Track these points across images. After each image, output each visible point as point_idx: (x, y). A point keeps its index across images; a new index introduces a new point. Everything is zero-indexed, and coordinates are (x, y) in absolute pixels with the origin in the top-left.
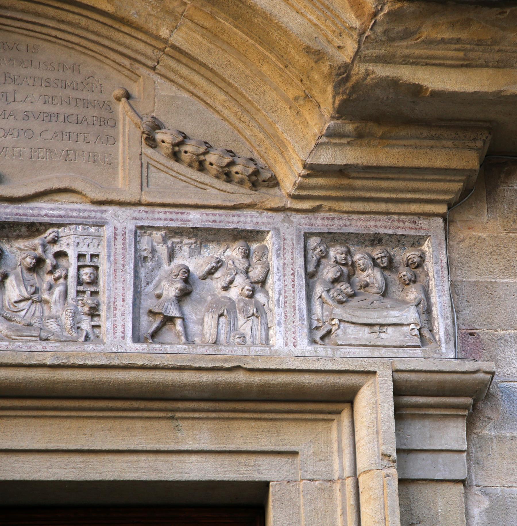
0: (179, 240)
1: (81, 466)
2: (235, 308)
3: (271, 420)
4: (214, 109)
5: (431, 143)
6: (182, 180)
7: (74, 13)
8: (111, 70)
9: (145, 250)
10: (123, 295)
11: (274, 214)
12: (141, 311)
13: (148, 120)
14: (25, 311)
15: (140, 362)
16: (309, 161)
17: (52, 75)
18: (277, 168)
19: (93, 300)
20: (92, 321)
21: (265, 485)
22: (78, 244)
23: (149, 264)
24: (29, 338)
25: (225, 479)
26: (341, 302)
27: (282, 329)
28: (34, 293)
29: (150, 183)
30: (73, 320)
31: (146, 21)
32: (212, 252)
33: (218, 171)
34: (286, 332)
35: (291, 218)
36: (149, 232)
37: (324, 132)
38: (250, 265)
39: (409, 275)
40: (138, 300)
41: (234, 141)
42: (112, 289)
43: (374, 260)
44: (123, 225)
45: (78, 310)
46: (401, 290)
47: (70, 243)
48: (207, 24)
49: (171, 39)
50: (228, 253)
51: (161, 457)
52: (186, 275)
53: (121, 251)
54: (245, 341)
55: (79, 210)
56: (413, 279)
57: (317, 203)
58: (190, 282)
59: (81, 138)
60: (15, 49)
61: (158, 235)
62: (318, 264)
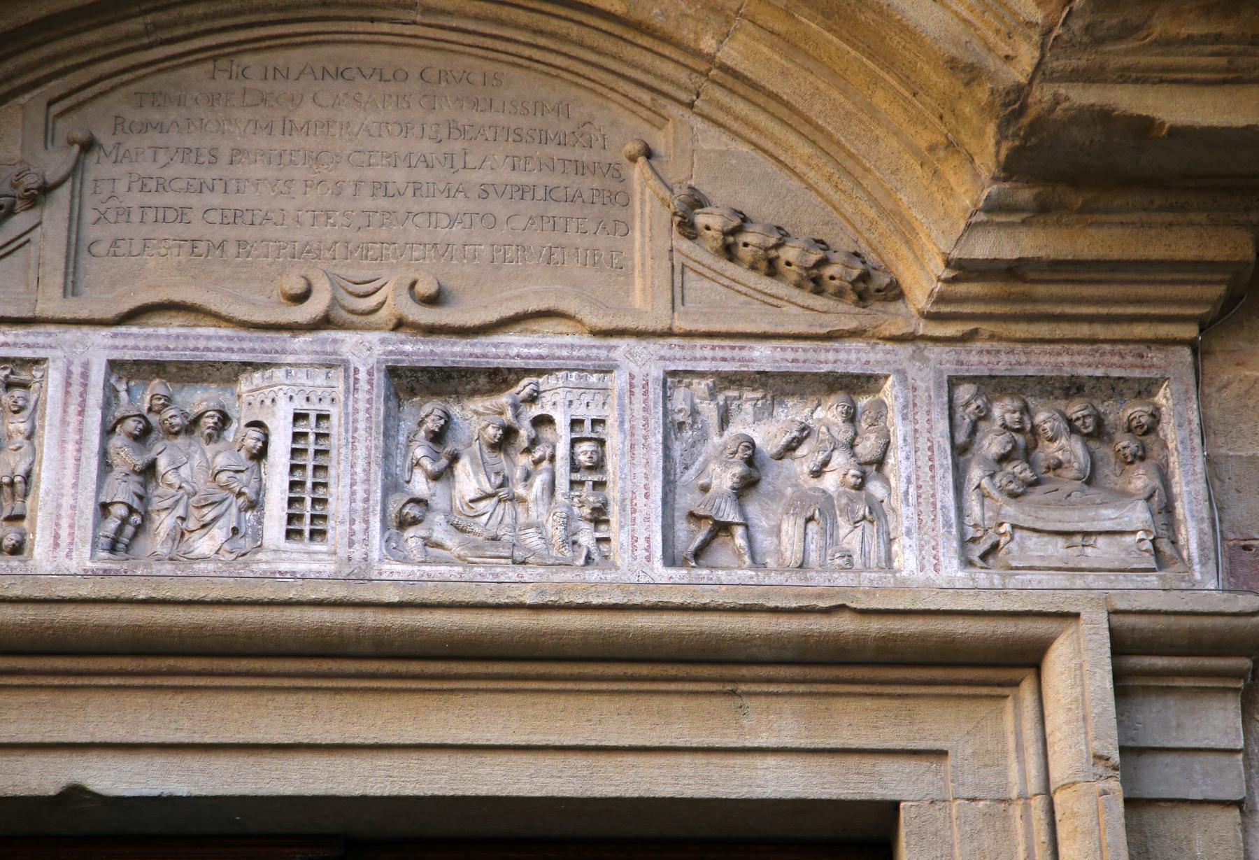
0: (736, 394)
1: (585, 773)
2: (833, 507)
3: (899, 696)
4: (792, 171)
5: (1169, 217)
6: (739, 292)
7: (558, 17)
8: (621, 110)
9: (680, 411)
10: (646, 487)
11: (897, 346)
12: (677, 514)
13: (681, 192)
14: (487, 516)
15: (678, 600)
16: (955, 254)
17: (523, 122)
18: (901, 267)
21: (893, 808)
22: (571, 402)
23: (688, 434)
25: (824, 797)
26: (1014, 495)
27: (914, 542)
28: (501, 486)
29: (687, 299)
30: (565, 529)
31: (678, 27)
32: (792, 413)
33: (801, 275)
34: (921, 548)
35: (926, 353)
36: (686, 381)
37: (981, 204)
38: (856, 434)
39: (1133, 446)
40: (670, 495)
41: (827, 224)
43: (1070, 422)
44: (645, 370)
45: (572, 513)
46: (1118, 472)
47: (559, 400)
48: (780, 27)
49: (719, 54)
50: (820, 413)
51: (715, 759)
52: (749, 452)
54: (851, 563)
55: (572, 346)
56: (1140, 453)
57: (969, 326)
58: (757, 464)
59: (573, 226)
60: (464, 80)
61: (701, 386)
62: (974, 430)
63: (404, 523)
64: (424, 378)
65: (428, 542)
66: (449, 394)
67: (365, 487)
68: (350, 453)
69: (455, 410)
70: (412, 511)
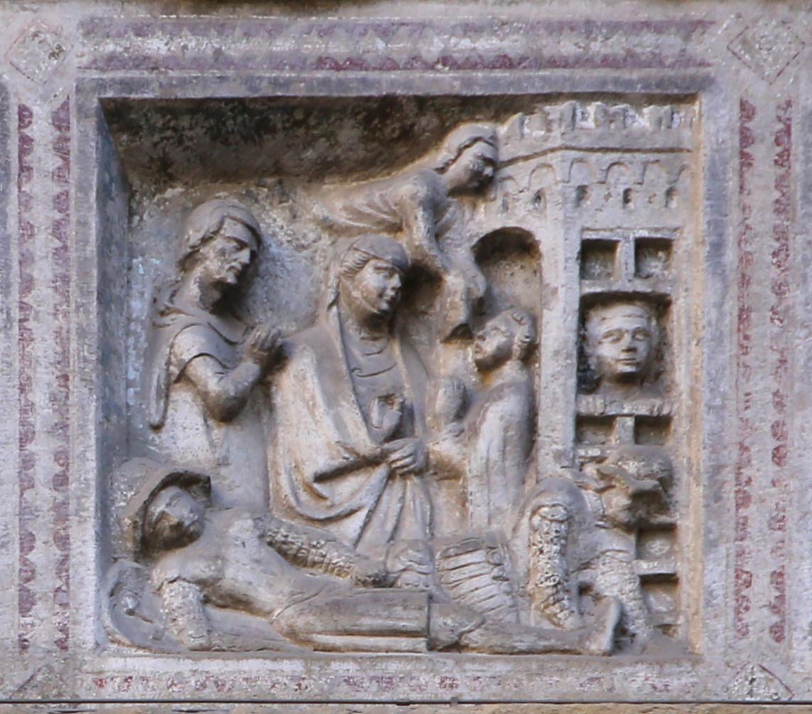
10: (778, 430)
14: (360, 517)
19: (647, 459)
20: (640, 555)
22: (582, 191)
24: (382, 641)
30: (562, 553)
42: (732, 404)
45: (581, 509)
53: (772, 219)
63: (154, 542)
64: (197, 132)
65: (215, 595)
66: (258, 174)
67: (57, 444)
68: (15, 351)
69: (274, 221)
70: (176, 509)
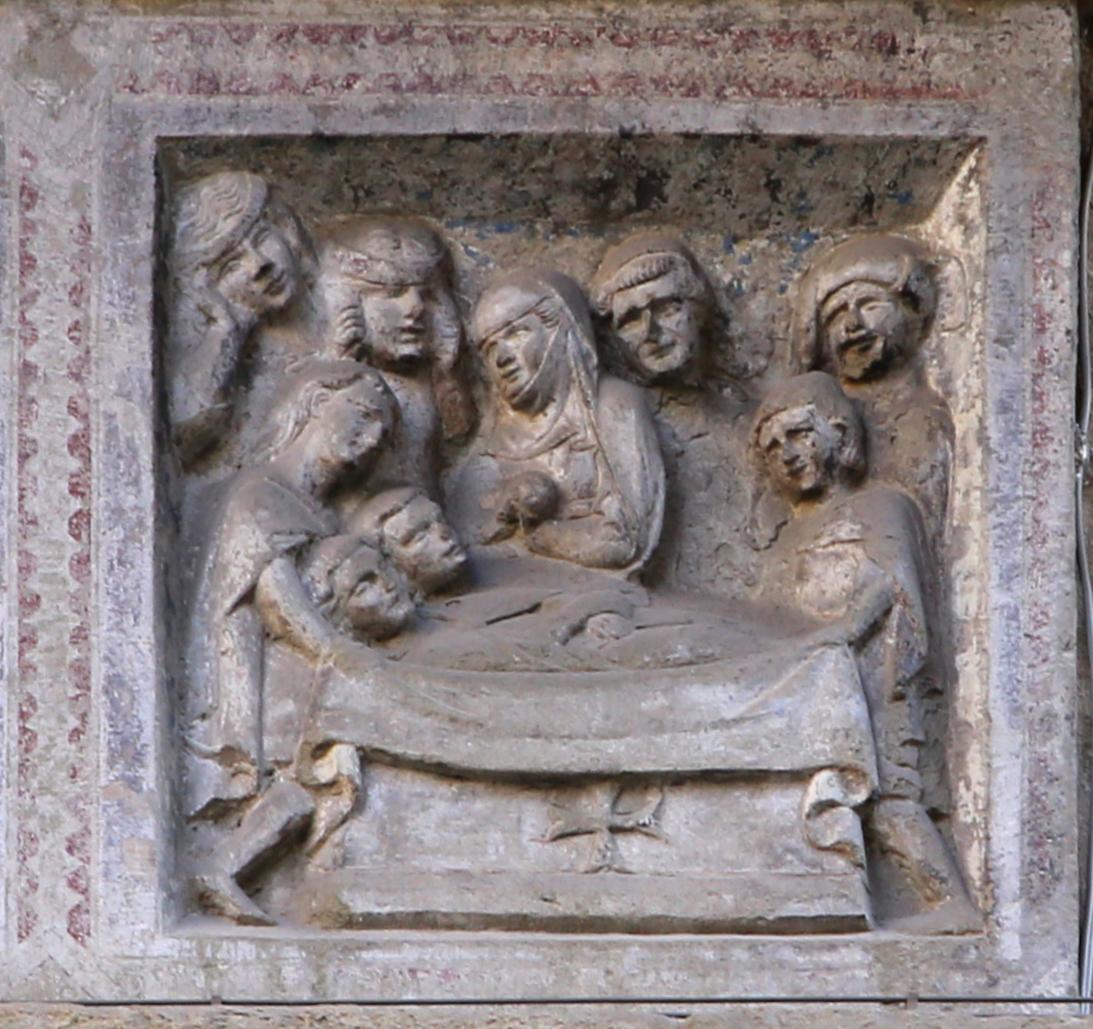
26: (377, 632)
39: (825, 426)
43: (601, 326)
46: (764, 532)
56: (849, 454)
